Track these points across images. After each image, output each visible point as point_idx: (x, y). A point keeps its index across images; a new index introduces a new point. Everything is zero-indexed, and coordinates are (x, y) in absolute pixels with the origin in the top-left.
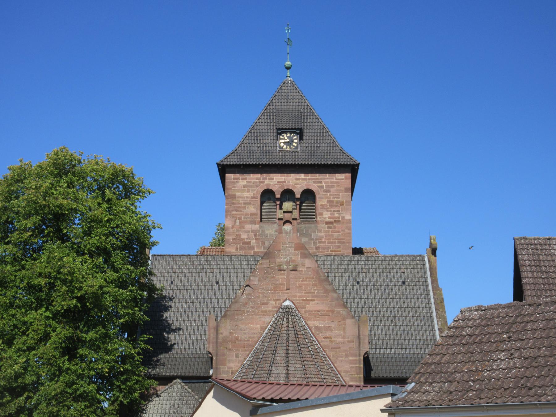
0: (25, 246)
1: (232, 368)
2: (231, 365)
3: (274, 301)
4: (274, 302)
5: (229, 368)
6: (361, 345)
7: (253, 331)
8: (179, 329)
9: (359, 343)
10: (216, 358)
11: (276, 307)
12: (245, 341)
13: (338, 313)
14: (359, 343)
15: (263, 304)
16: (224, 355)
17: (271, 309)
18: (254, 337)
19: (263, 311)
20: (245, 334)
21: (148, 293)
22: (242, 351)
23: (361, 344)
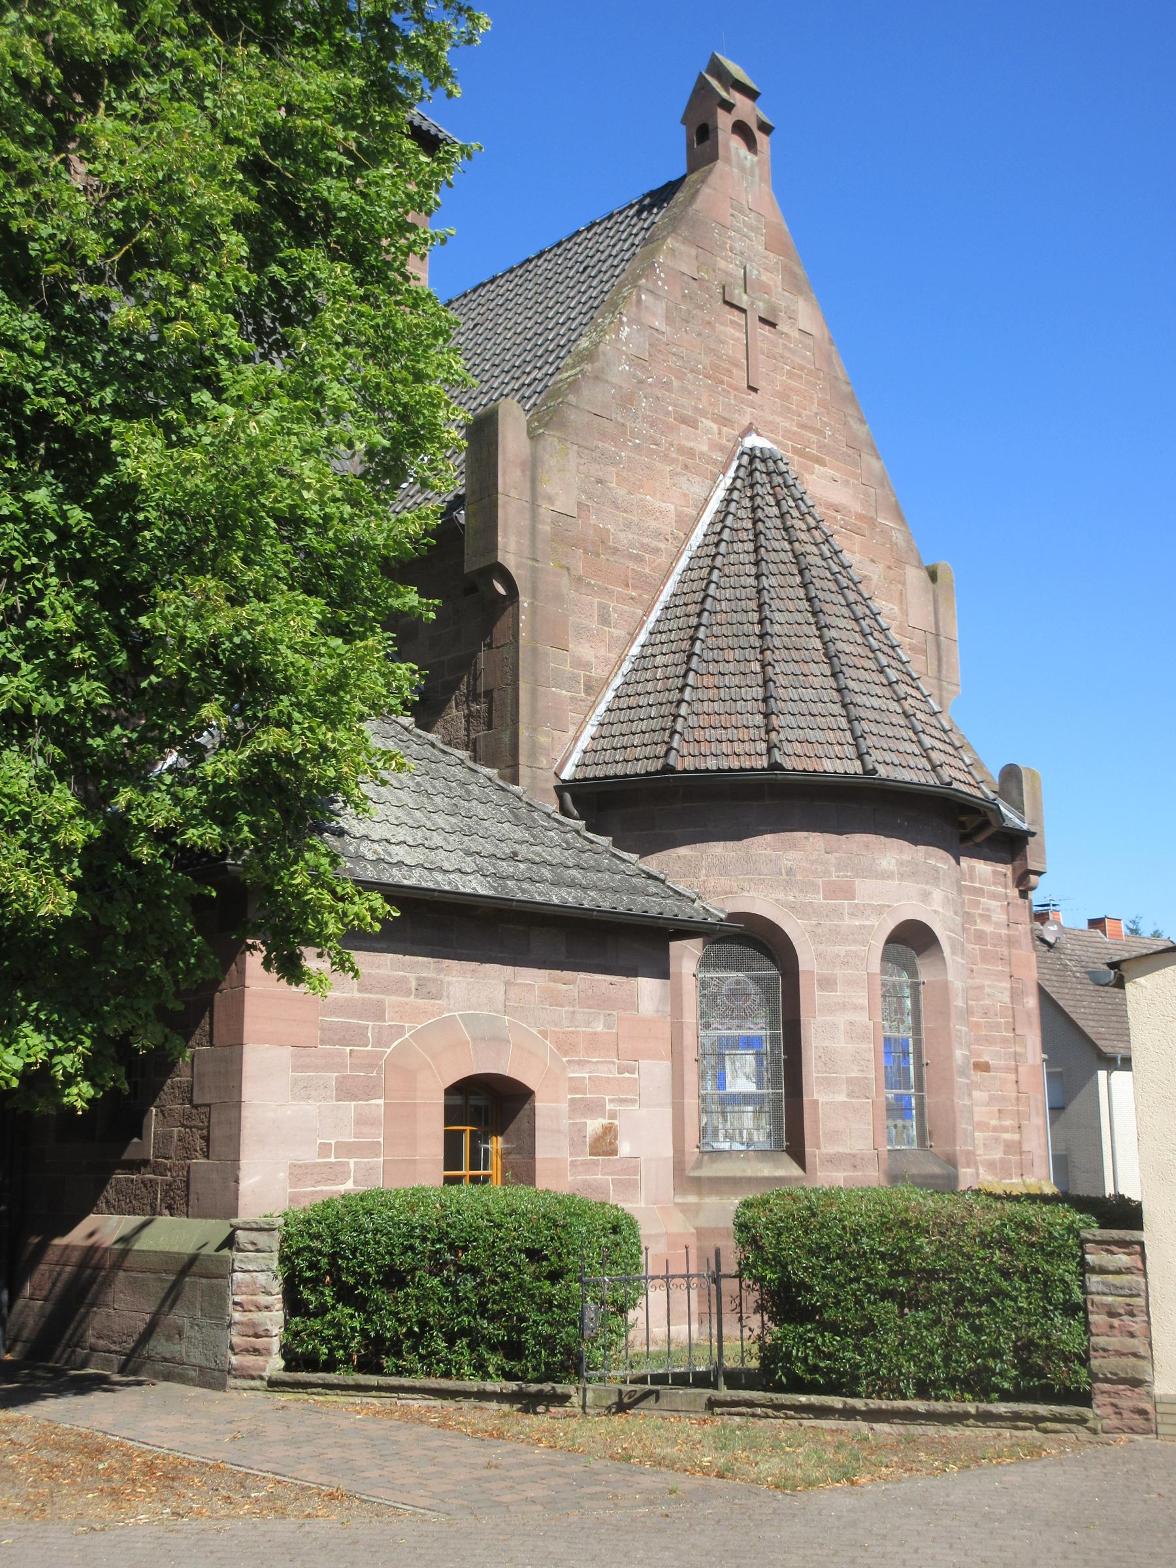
0: (751, 462)
1: (587, 665)
2: (585, 651)
3: (714, 420)
4: (715, 427)
5: (580, 663)
6: (944, 672)
7: (653, 524)
8: (718, 1253)
9: (939, 660)
10: (532, 604)
11: (722, 449)
12: (630, 556)
13: (885, 532)
14: (939, 660)
15: (684, 420)
16: (558, 598)
17: (705, 448)
18: (657, 550)
19: (681, 450)
20: (628, 525)
21: (65, 926)
22: (622, 599)
23: (944, 666)
